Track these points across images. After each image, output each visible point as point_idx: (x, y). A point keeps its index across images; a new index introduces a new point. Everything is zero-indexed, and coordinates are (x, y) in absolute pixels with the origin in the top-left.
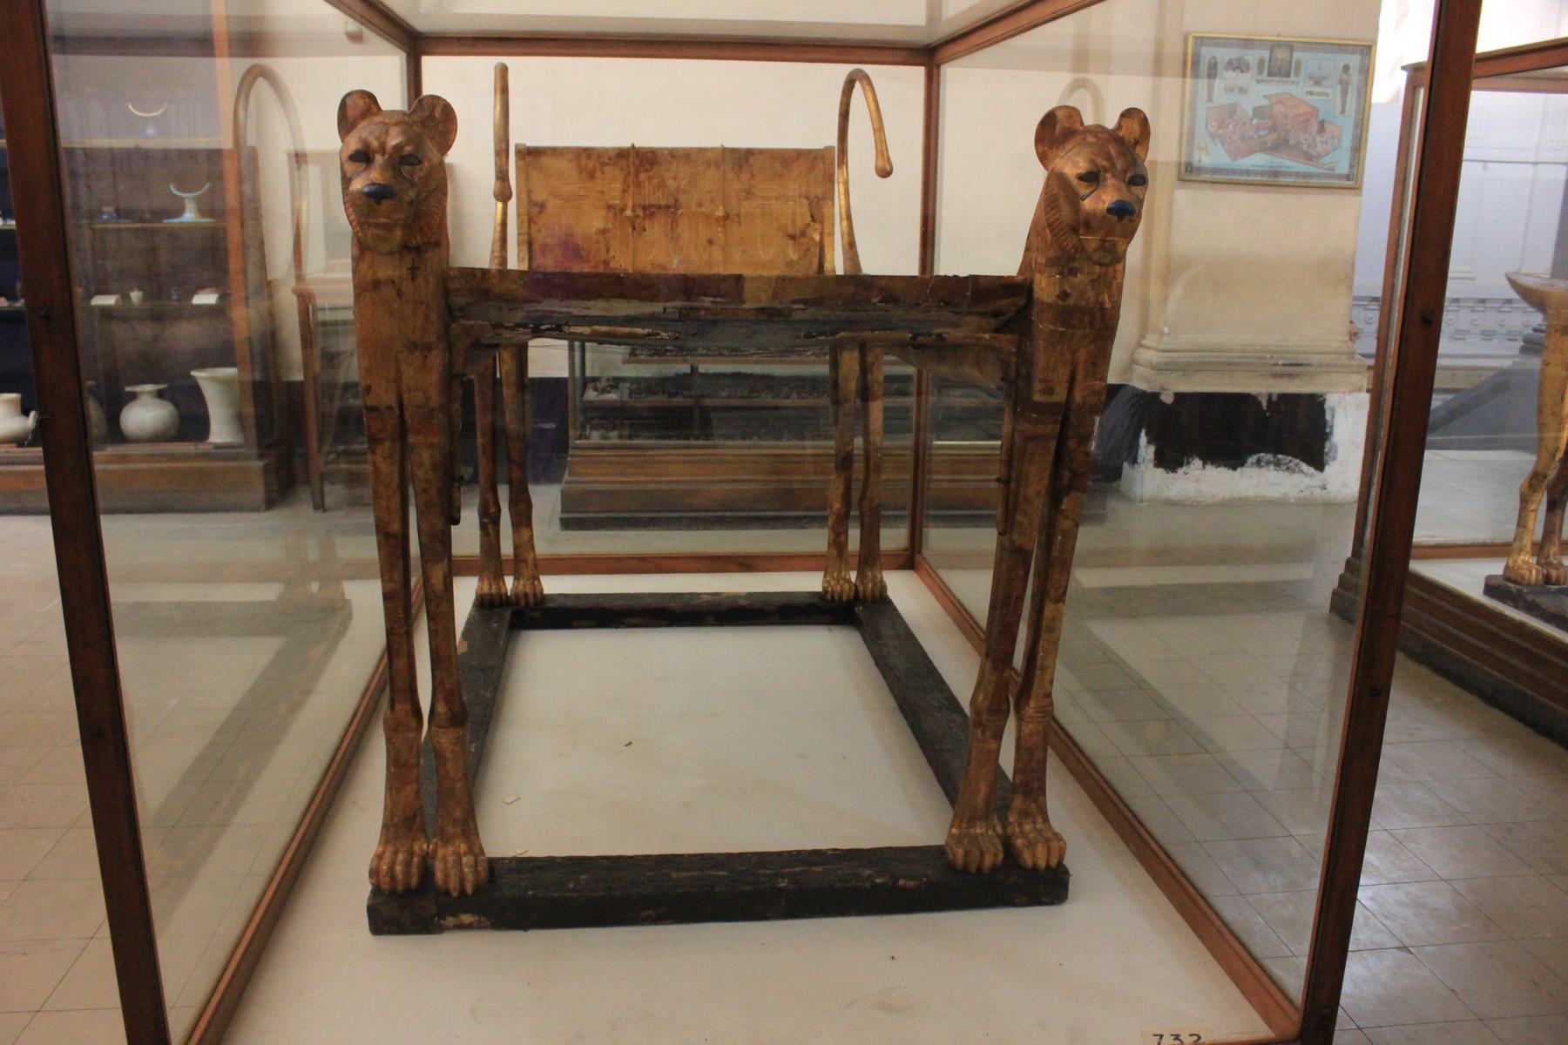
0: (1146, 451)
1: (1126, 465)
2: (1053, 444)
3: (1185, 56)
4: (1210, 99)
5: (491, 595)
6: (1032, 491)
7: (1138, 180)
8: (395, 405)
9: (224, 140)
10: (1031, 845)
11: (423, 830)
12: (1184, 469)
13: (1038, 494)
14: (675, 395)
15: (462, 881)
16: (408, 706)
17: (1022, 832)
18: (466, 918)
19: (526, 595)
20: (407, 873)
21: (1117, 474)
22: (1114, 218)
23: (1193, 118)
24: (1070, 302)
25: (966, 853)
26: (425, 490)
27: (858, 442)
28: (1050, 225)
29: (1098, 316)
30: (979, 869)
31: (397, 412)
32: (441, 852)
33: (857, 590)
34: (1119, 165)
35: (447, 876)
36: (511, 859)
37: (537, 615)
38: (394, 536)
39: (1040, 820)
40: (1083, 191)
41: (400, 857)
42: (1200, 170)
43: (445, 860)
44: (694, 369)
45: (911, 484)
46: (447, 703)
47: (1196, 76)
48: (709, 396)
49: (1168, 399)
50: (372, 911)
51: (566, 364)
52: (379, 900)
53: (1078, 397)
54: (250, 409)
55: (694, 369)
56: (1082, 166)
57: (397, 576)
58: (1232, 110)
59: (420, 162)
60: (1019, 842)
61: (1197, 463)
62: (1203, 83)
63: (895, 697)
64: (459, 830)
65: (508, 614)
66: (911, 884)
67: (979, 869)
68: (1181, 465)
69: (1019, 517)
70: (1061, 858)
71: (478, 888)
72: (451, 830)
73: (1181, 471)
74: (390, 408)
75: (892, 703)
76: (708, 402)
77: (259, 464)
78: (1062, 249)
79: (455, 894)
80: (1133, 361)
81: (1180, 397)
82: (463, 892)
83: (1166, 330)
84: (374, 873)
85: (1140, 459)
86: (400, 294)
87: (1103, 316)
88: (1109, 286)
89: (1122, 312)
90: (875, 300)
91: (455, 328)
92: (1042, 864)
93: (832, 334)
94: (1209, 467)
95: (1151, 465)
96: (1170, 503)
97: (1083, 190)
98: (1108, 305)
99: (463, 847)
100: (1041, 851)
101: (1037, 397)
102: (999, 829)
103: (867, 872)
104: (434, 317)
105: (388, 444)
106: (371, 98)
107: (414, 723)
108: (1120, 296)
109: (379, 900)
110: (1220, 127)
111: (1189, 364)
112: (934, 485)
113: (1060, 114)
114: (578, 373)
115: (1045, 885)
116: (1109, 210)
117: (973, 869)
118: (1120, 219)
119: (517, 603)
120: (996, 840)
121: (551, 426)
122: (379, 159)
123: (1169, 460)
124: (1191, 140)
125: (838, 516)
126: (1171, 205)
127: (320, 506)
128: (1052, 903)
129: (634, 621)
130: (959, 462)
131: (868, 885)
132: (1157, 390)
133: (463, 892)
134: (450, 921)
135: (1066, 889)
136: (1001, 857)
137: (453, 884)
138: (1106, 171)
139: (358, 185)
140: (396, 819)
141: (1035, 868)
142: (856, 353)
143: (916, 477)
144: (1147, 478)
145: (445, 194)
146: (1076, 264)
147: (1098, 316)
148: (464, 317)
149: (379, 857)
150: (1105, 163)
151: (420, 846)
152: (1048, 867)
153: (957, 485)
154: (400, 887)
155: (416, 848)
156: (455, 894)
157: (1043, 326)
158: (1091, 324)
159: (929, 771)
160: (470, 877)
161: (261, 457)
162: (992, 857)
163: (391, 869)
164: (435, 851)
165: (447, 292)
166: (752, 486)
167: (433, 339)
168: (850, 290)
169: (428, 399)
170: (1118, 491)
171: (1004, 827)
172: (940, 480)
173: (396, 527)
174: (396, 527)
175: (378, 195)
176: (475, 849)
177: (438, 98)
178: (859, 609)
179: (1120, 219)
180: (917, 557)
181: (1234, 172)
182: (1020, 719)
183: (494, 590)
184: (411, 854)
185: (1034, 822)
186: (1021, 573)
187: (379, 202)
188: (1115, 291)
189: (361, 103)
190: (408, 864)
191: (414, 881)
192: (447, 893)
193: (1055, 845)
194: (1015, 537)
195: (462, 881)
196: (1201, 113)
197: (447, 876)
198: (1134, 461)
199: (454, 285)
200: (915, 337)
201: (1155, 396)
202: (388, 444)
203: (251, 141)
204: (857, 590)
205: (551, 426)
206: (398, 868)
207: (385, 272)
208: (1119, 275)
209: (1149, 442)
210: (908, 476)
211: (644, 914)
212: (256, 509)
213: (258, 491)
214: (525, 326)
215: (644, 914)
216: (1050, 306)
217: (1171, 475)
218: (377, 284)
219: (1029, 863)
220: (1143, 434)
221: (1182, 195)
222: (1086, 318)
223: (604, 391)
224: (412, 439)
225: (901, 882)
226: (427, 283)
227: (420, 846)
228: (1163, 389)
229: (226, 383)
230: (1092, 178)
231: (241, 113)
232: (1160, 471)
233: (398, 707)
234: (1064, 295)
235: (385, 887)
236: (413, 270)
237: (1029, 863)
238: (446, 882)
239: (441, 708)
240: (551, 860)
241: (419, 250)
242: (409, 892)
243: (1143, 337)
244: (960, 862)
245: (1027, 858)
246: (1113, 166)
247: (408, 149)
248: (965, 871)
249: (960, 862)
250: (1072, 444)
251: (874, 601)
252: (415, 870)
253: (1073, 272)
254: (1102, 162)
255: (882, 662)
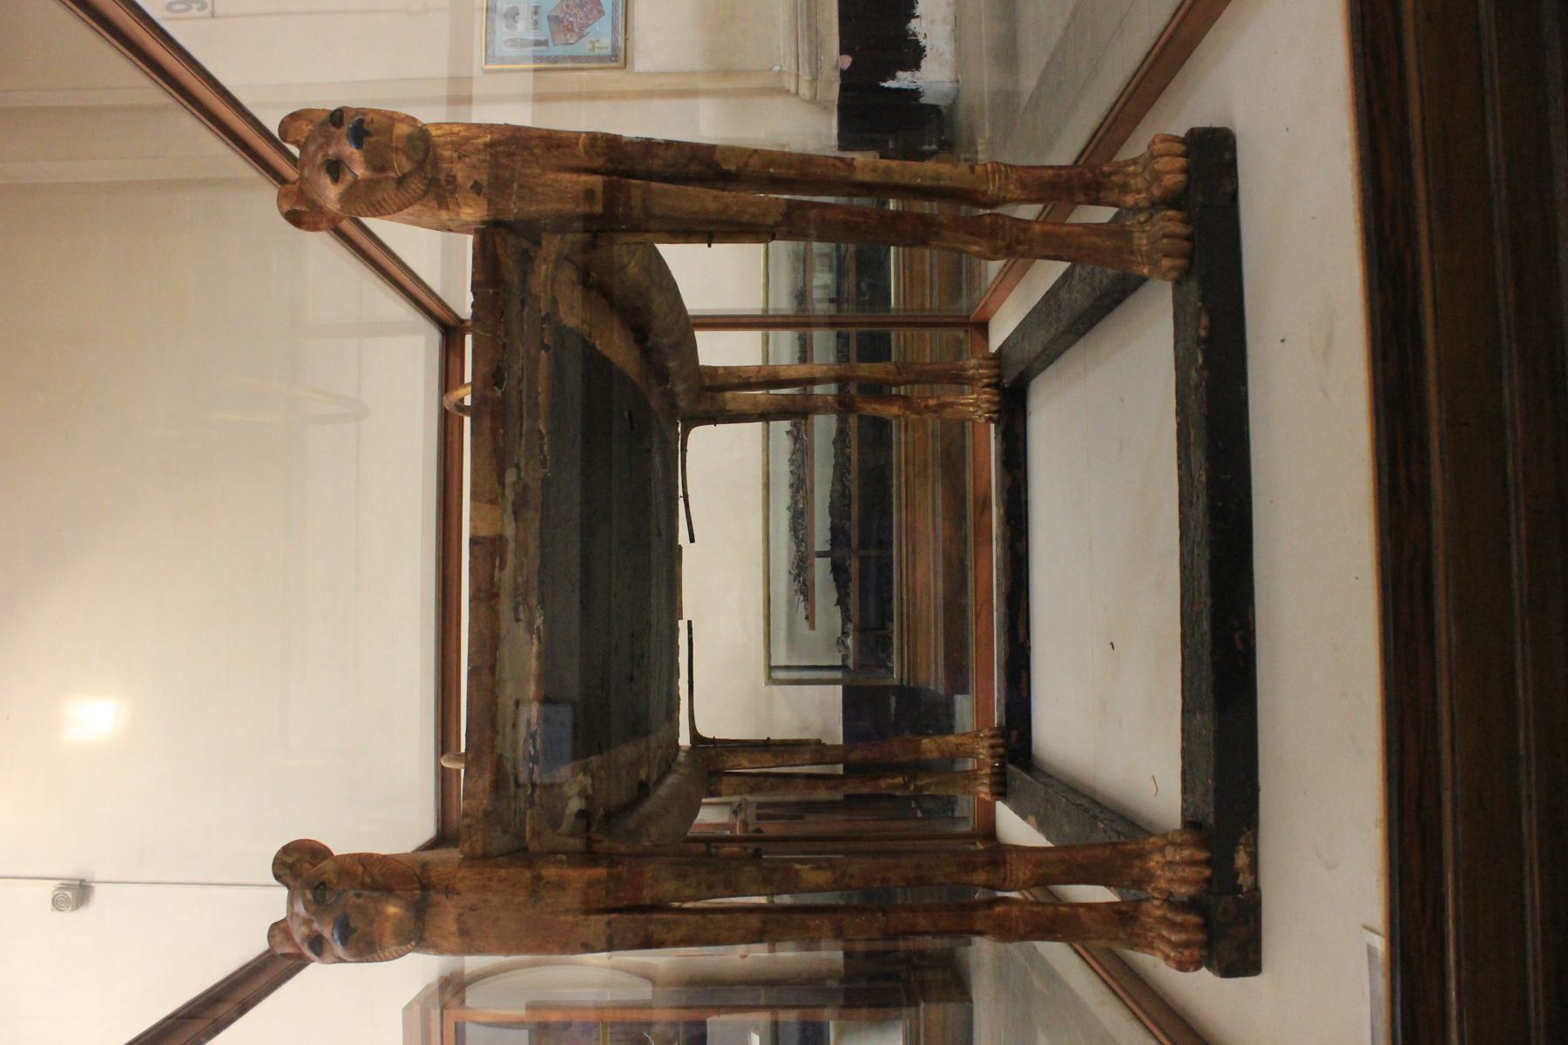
0: (903, 80)
1: (923, 100)
2: (654, 185)
3: (536, 70)
4: (545, 43)
5: (991, 784)
6: (712, 206)
7: (337, 117)
8: (606, 917)
9: (523, 1036)
10: (1157, 176)
11: (1139, 901)
12: (920, 38)
13: (716, 198)
14: (850, 580)
15: (1191, 863)
16: (981, 913)
17: (1148, 189)
18: (1241, 859)
19: (992, 747)
20: (1181, 927)
21: (935, 109)
22: (368, 140)
23: (564, 59)
24: (484, 178)
25: (1166, 255)
26: (710, 887)
27: (818, 390)
28: (400, 209)
29: (500, 149)
30: (1188, 238)
31: (613, 916)
32: (1162, 884)
33: (988, 386)
34: (321, 140)
35: (1184, 881)
36: (1184, 800)
37: (1014, 734)
38: (764, 923)
39: (1131, 169)
40: (349, 178)
41: (1165, 933)
42: (614, 48)
43: (1170, 881)
44: (821, 555)
45: (937, 332)
46: (974, 870)
47: (538, 59)
48: (849, 540)
49: (847, 61)
50: (1228, 972)
51: (831, 687)
52: (1215, 963)
53: (599, 162)
54: (864, 1012)
55: (821, 555)
56: (326, 180)
57: (816, 921)
58: (554, 20)
59: (323, 883)
60: (1156, 192)
61: (914, 25)
62: (529, 51)
63: (1069, 346)
64: (1137, 863)
65: (1011, 767)
66: (1204, 321)
67: (1188, 238)
68: (917, 42)
69: (746, 218)
70: (1175, 139)
71: (1204, 844)
72: (1136, 870)
73: (923, 42)
74: (609, 923)
75: (1081, 343)
76: (855, 542)
77: (923, 1005)
78: (426, 193)
79: (1207, 872)
80: (813, 100)
81: (843, 51)
82: (1207, 863)
83: (777, 68)
84: (1182, 966)
85: (913, 86)
86: (473, 908)
87: (500, 143)
88: (467, 140)
89: (501, 121)
90: (499, 393)
91: (533, 846)
92: (1180, 162)
93: (542, 438)
94: (918, 11)
95: (917, 74)
96: (958, 53)
97: (349, 178)
98: (488, 139)
99: (1157, 858)
100: (1162, 164)
101: (598, 208)
102: (1142, 218)
103: (1194, 374)
104: (503, 871)
105: (652, 927)
106: (275, 926)
107: (999, 909)
108: (479, 126)
109: (1215, 963)
110: (571, 30)
111: (810, 41)
112: (936, 304)
113: (287, 208)
114: (838, 675)
115: (1213, 154)
116: (359, 145)
117: (1186, 245)
118: (368, 134)
119: (1000, 756)
120: (1157, 217)
121: (893, 700)
122: (316, 926)
123: (913, 55)
124: (588, 59)
125: (907, 408)
126: (650, 74)
127: (969, 943)
128: (1232, 148)
129: (1022, 632)
130: (912, 278)
131: (1205, 374)
132: (837, 74)
133: (1207, 863)
134: (1244, 880)
135: (1212, 131)
136: (1170, 213)
137: (1188, 872)
138: (326, 154)
139: (339, 950)
140: (1122, 935)
141: (1185, 171)
142: (729, 395)
143: (910, 324)
144: (932, 77)
145: (370, 856)
146: (442, 177)
147: (500, 149)
148: (520, 836)
149: (1167, 958)
150: (320, 155)
151: (1155, 909)
152: (1186, 155)
153: (936, 278)
154: (1200, 937)
155: (1159, 913)
156: (1207, 872)
157: (514, 209)
158: (510, 155)
159: (1131, 301)
160: (1186, 853)
161: (917, 1005)
162: (1170, 223)
163: (1175, 946)
164: (1161, 891)
165: (486, 856)
166: (939, 494)
167: (528, 874)
168: (486, 422)
169: (599, 881)
170: (952, 108)
171: (1141, 210)
172: (932, 302)
173: (754, 921)
174: (754, 921)
175: (346, 933)
176: (1167, 839)
177: (276, 858)
178: (1006, 382)
179: (368, 134)
180: (972, 319)
181: (615, 11)
182: (1004, 201)
183: (986, 781)
184: (1164, 919)
185: (1135, 175)
186: (813, 214)
187: (354, 931)
188: (474, 132)
189: (279, 938)
190: (1173, 926)
191: (1193, 919)
192: (1208, 881)
193: (1159, 147)
194: (770, 220)
195: (1191, 863)
196: (558, 51)
197: (1184, 881)
198: (915, 93)
199: (479, 849)
200: (546, 348)
201: (843, 73)
202: (652, 927)
203: (520, 1013)
204: (988, 386)
205: (893, 700)
206: (1174, 938)
207: (452, 926)
208: (456, 129)
209: (893, 77)
210: (927, 333)
211: (1240, 646)
212: (970, 1011)
213: (952, 1009)
214: (531, 772)
215: (1240, 646)
216: (490, 202)
217: (928, 51)
218: (464, 932)
219: (1181, 178)
220: (886, 85)
221: (641, 63)
222: (503, 161)
223: (847, 648)
224: (648, 902)
225: (1203, 333)
226: (463, 878)
227: (1155, 909)
228: (836, 67)
229: (841, 1033)
230: (335, 168)
231: (482, 1019)
232: (923, 63)
233: (979, 926)
234: (477, 188)
235: (1197, 953)
236: (449, 891)
237: (1181, 178)
238: (1196, 882)
239: (980, 877)
240: (1184, 751)
241: (425, 887)
242: (1206, 927)
243: (788, 91)
244: (1179, 262)
245: (1173, 180)
246: (321, 147)
247: (309, 895)
248: (1190, 256)
249: (1179, 262)
250: (657, 164)
251: (999, 367)
252: (1179, 918)
253: (451, 179)
254: (319, 159)
255: (1050, 355)
